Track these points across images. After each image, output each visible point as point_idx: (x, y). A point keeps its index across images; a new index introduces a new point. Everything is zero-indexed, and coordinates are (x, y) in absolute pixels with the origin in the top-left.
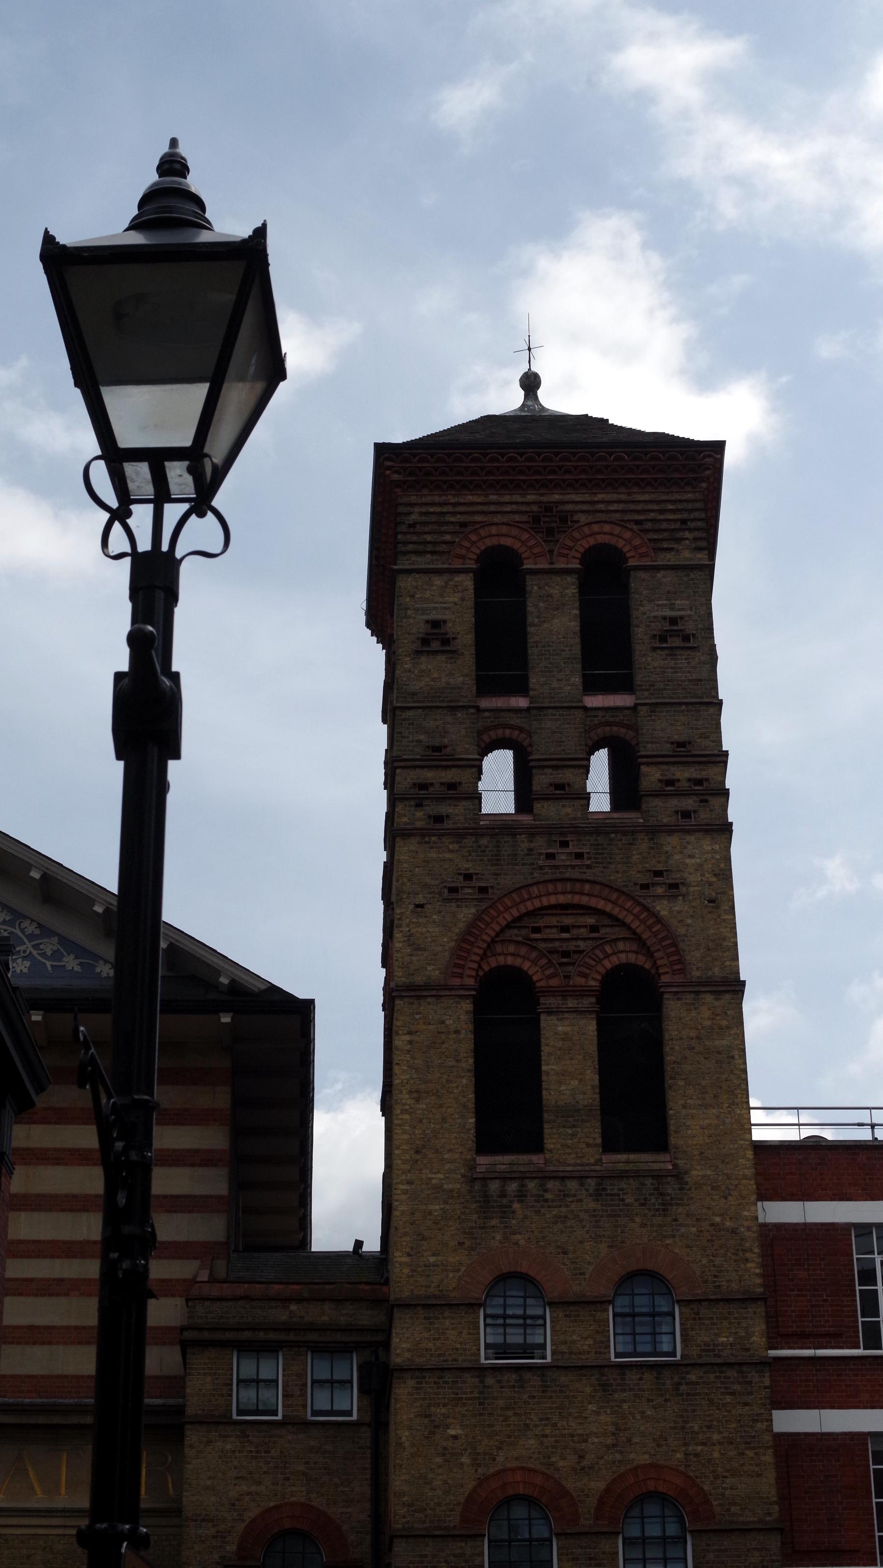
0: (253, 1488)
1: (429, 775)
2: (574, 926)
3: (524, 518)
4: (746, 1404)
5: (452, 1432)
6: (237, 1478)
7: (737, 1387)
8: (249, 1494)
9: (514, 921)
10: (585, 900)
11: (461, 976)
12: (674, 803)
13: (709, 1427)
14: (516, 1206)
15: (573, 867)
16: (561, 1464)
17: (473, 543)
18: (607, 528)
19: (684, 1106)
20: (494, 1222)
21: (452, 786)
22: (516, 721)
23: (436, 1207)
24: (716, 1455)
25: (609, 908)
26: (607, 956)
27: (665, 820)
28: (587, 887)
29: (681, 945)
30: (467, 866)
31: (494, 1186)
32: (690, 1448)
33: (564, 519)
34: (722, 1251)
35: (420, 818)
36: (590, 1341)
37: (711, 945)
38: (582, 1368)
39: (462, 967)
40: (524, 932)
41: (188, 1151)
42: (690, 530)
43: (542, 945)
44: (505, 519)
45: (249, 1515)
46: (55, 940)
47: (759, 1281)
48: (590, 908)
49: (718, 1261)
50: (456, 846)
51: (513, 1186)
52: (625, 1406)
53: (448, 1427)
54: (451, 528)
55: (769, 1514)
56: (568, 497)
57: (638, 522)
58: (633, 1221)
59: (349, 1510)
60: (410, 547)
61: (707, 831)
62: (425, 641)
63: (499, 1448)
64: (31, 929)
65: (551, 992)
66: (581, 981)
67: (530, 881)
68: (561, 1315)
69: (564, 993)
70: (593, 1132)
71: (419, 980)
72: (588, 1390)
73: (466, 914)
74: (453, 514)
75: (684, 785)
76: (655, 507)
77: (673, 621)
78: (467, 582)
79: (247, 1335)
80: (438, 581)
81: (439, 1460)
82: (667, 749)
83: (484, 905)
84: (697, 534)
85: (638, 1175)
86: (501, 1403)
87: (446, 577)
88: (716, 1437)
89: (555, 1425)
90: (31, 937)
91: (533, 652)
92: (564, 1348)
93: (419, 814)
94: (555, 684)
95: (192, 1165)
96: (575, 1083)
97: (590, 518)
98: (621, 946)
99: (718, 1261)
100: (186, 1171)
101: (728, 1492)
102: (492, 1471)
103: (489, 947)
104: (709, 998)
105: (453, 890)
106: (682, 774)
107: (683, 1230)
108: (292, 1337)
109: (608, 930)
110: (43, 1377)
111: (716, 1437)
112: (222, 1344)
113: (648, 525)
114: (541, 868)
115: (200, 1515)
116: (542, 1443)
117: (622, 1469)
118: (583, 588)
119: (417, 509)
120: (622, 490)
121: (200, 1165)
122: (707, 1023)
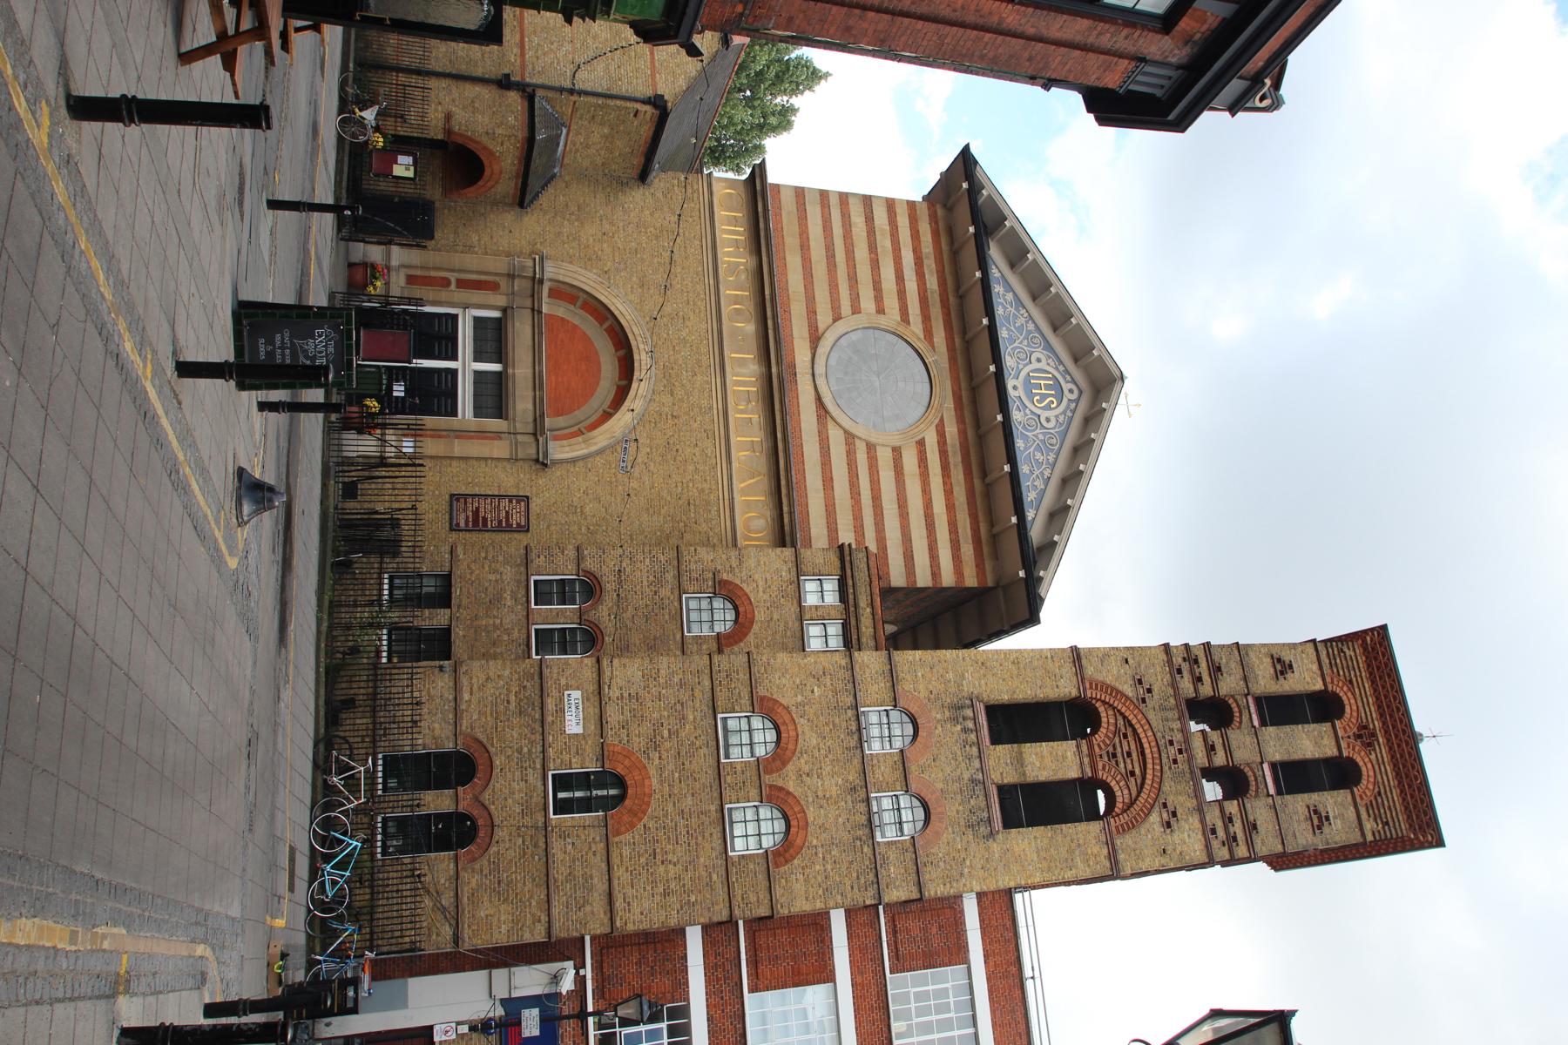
0: (761, 589)
1: (1203, 664)
2: (1132, 760)
3: (1364, 721)
4: (852, 888)
5: (816, 690)
7: (862, 881)
9: (1129, 721)
10: (1150, 766)
11: (1091, 688)
12: (1219, 824)
13: (835, 862)
14: (959, 728)
15: (1168, 757)
16: (802, 761)
17: (1342, 689)
18: (1371, 773)
19: (1035, 837)
20: (947, 714)
21: (1200, 679)
22: (1245, 718)
23: (951, 676)
24: (818, 867)
25: (1148, 782)
26: (1118, 783)
27: (1207, 818)
28: (1158, 767)
29: (1134, 831)
30: (1155, 689)
31: (969, 713)
32: (820, 849)
33: (1370, 745)
34: (948, 867)
35: (1178, 660)
36: (881, 779)
37: (1138, 852)
38: (865, 773)
39: (1097, 688)
40: (1123, 730)
42: (1383, 828)
43: (1117, 740)
44: (1361, 709)
45: (744, 586)
46: (1043, 487)
47: (932, 893)
48: (1145, 769)
49: (941, 864)
50: (1166, 683)
51: (970, 725)
52: (843, 803)
53: (819, 686)
54: (1347, 674)
55: (782, 907)
56: (1382, 747)
57: (1379, 793)
58: (960, 805)
60: (1330, 650)
61: (1207, 846)
62: (1279, 660)
63: (809, 720)
64: (1047, 473)
65: (1091, 747)
66: (1100, 767)
67: (1155, 730)
68: (896, 759)
69: (1091, 755)
70: (1010, 778)
71: (1084, 662)
72: (851, 778)
73: (1129, 691)
74: (1356, 676)
75: (1232, 830)
76: (1391, 804)
77: (1327, 818)
78: (1319, 686)
79: (850, 582)
80: (1315, 667)
81: (798, 682)
82: (1251, 818)
83: (1135, 701)
84: (1382, 832)
85: (988, 807)
86: (837, 721)
87: (1319, 672)
88: (829, 867)
89: (827, 757)
90: (1042, 473)
91: (1287, 728)
92: (875, 761)
93: (1180, 660)
94: (1272, 743)
96: (1038, 764)
97: (1374, 762)
98: (1126, 792)
99: (941, 864)
101: (794, 877)
102: (794, 715)
103: (1111, 705)
104: (1105, 851)
105: (1140, 682)
106: (1237, 828)
107: (958, 839)
108: (852, 609)
109: (1134, 782)
110: (805, 486)
111: (829, 867)
112: (843, 568)
113: (1380, 800)
114: (1164, 737)
116: (814, 748)
117: (802, 803)
118: (1327, 761)
119: (1352, 654)
120: (1396, 783)
122: (1090, 852)
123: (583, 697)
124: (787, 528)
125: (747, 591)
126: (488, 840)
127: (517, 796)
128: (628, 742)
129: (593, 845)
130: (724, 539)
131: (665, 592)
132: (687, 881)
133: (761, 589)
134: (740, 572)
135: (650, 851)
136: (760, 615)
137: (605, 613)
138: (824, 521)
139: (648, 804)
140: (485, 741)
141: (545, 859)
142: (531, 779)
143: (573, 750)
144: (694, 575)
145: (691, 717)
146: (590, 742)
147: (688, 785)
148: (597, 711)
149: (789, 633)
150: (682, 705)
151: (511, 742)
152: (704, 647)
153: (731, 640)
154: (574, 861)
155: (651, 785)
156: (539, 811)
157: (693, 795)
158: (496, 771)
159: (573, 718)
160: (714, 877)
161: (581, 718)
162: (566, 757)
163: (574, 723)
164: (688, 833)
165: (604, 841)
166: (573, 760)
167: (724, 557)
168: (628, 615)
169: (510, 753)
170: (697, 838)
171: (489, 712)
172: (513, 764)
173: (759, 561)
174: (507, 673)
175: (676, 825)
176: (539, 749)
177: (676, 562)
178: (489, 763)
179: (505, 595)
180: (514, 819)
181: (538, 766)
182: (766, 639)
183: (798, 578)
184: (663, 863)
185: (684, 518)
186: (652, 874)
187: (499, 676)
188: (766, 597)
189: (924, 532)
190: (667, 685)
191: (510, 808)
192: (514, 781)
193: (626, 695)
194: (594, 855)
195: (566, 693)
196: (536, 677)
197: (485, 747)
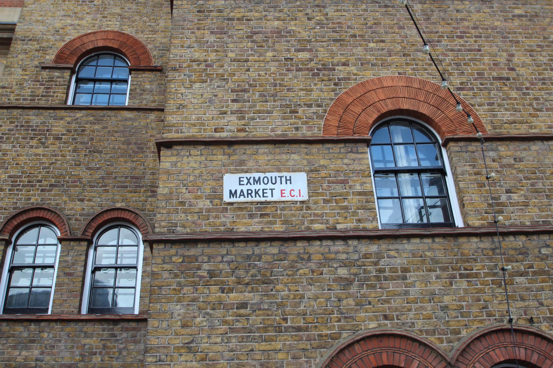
0: (76, 22)
6: (64, 16)
8: (71, 25)
59: (154, 36)
115: (28, 37)
123: (237, 171)
125: (76, 35)
126: (530, 341)
127: (436, 287)
128: (319, 106)
129: (505, 161)
131: (59, 127)
132: (533, 43)
133: (76, 22)
134: (48, 41)
135: (498, 84)
136: (114, 25)
137: (78, 206)
139: (423, 83)
140: (328, 353)
141: (546, 238)
142: (399, 262)
143: (339, 188)
144: (41, 90)
145: (276, 23)
146: (322, 162)
147: (386, 33)
148: (263, 149)
150: (256, 33)
151: (328, 299)
152: (148, 87)
153: (142, 57)
154: (536, 191)
155: (392, 79)
156: (459, 247)
157: (402, 28)
158: (389, 327)
159: (278, 187)
160: (517, 12)
161: (277, 174)
162: (354, 200)
163: (288, 187)
164: (461, 37)
165: (494, 144)
166: (358, 188)
168: (85, 175)
169: (351, 301)
170: (468, 27)
171: (264, 346)
172: (372, 295)
173: (38, 21)
174: (178, 309)
175: (452, 50)
176: (339, 246)
177: (15, 112)
178: (374, 343)
179: (19, 359)
180: (480, 291)
181: (373, 248)
182: (145, 22)
183: (72, 109)
184: (513, 69)
186: (532, 84)
187: (184, 326)
188: (89, 18)
190: (222, 49)
191: (461, 299)
192: (407, 293)
193: (235, 106)
194: (521, 160)
195: (227, 198)
196: (193, 251)
197: (342, 351)
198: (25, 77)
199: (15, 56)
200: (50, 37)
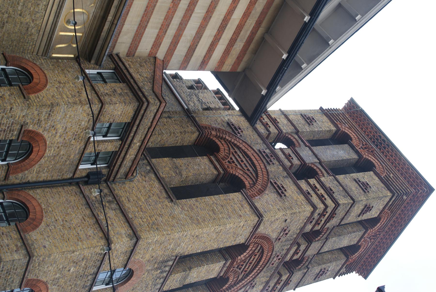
41: (211, 55)
59: (35, 173)
95: (205, 57)
100: (204, 54)
121: (204, 59)
124: (103, 34)
130: (41, 33)
133: (58, 134)
138: (139, 19)
149: (68, 163)
167: (36, 113)
173: (66, 115)
185: (11, 10)
189: (214, 32)
198: (17, 118)
199: (38, 109)
200: (49, 124)
